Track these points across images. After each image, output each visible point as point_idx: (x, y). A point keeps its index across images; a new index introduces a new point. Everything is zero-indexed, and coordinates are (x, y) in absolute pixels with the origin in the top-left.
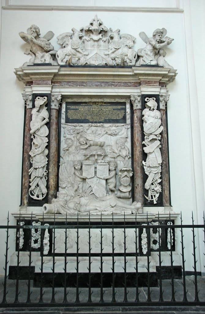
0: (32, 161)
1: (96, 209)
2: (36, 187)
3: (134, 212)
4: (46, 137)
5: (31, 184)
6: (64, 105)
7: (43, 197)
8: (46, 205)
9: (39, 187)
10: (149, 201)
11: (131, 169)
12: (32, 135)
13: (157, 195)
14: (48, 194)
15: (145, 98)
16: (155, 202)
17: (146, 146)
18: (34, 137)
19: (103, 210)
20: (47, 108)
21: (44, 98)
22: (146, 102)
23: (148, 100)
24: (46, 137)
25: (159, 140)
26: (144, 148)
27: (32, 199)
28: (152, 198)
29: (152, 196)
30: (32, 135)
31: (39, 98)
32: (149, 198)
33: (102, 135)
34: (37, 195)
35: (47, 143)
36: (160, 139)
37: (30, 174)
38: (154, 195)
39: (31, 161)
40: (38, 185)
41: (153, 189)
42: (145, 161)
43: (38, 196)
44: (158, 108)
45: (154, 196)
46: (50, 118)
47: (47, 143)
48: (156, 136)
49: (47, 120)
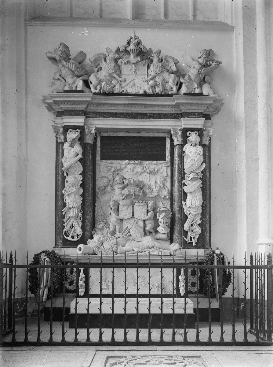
0: (66, 200)
1: (134, 250)
2: (70, 227)
3: (172, 253)
4: (80, 174)
5: (65, 225)
6: (99, 140)
7: (78, 238)
8: (81, 246)
9: (74, 227)
10: (188, 243)
11: (170, 210)
12: (65, 172)
13: (197, 237)
14: (83, 235)
15: (187, 132)
16: (194, 244)
17: (186, 185)
18: (67, 175)
19: (140, 251)
20: (80, 142)
21: (77, 131)
22: (188, 137)
23: (190, 134)
24: (80, 174)
25: (200, 178)
26: (185, 188)
27: (67, 240)
28: (191, 240)
29: (191, 238)
30: (65, 172)
31: (71, 131)
32: (188, 240)
33: (140, 173)
34: (72, 235)
35: (81, 181)
36: (201, 178)
37: (63, 214)
38: (193, 236)
39: (65, 200)
40: (73, 226)
41: (193, 231)
42: (185, 201)
43: (73, 237)
44: (201, 144)
45: (194, 238)
46: (84, 154)
47: (81, 181)
48: (198, 174)
49: (80, 156)
